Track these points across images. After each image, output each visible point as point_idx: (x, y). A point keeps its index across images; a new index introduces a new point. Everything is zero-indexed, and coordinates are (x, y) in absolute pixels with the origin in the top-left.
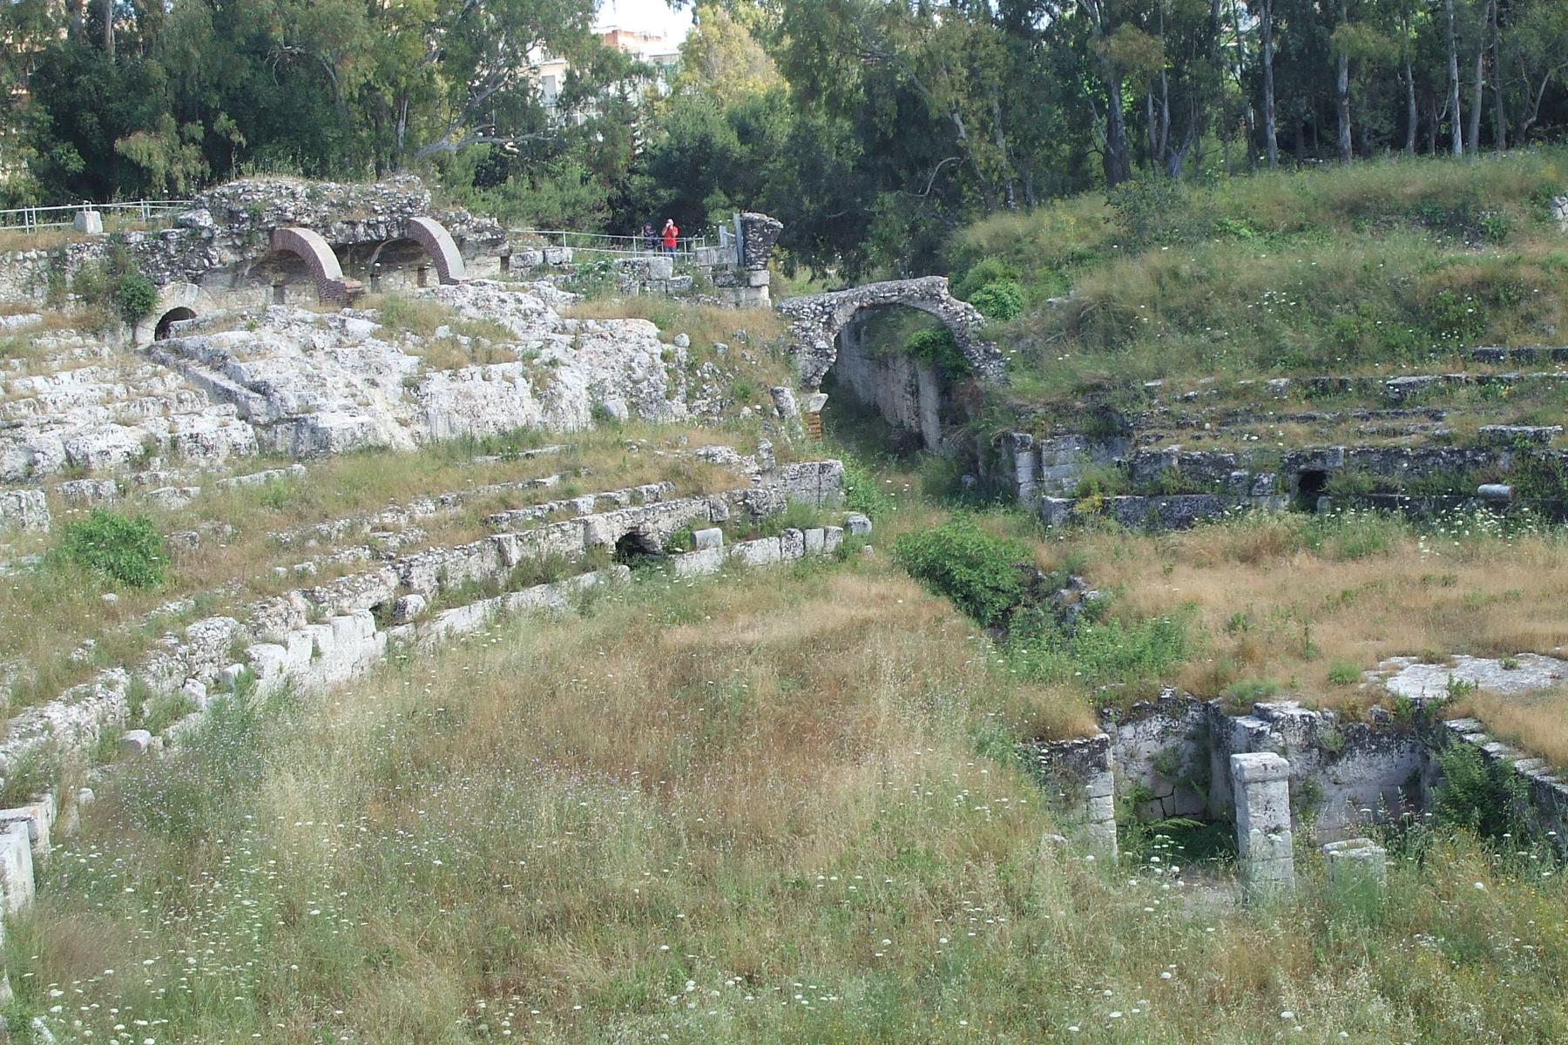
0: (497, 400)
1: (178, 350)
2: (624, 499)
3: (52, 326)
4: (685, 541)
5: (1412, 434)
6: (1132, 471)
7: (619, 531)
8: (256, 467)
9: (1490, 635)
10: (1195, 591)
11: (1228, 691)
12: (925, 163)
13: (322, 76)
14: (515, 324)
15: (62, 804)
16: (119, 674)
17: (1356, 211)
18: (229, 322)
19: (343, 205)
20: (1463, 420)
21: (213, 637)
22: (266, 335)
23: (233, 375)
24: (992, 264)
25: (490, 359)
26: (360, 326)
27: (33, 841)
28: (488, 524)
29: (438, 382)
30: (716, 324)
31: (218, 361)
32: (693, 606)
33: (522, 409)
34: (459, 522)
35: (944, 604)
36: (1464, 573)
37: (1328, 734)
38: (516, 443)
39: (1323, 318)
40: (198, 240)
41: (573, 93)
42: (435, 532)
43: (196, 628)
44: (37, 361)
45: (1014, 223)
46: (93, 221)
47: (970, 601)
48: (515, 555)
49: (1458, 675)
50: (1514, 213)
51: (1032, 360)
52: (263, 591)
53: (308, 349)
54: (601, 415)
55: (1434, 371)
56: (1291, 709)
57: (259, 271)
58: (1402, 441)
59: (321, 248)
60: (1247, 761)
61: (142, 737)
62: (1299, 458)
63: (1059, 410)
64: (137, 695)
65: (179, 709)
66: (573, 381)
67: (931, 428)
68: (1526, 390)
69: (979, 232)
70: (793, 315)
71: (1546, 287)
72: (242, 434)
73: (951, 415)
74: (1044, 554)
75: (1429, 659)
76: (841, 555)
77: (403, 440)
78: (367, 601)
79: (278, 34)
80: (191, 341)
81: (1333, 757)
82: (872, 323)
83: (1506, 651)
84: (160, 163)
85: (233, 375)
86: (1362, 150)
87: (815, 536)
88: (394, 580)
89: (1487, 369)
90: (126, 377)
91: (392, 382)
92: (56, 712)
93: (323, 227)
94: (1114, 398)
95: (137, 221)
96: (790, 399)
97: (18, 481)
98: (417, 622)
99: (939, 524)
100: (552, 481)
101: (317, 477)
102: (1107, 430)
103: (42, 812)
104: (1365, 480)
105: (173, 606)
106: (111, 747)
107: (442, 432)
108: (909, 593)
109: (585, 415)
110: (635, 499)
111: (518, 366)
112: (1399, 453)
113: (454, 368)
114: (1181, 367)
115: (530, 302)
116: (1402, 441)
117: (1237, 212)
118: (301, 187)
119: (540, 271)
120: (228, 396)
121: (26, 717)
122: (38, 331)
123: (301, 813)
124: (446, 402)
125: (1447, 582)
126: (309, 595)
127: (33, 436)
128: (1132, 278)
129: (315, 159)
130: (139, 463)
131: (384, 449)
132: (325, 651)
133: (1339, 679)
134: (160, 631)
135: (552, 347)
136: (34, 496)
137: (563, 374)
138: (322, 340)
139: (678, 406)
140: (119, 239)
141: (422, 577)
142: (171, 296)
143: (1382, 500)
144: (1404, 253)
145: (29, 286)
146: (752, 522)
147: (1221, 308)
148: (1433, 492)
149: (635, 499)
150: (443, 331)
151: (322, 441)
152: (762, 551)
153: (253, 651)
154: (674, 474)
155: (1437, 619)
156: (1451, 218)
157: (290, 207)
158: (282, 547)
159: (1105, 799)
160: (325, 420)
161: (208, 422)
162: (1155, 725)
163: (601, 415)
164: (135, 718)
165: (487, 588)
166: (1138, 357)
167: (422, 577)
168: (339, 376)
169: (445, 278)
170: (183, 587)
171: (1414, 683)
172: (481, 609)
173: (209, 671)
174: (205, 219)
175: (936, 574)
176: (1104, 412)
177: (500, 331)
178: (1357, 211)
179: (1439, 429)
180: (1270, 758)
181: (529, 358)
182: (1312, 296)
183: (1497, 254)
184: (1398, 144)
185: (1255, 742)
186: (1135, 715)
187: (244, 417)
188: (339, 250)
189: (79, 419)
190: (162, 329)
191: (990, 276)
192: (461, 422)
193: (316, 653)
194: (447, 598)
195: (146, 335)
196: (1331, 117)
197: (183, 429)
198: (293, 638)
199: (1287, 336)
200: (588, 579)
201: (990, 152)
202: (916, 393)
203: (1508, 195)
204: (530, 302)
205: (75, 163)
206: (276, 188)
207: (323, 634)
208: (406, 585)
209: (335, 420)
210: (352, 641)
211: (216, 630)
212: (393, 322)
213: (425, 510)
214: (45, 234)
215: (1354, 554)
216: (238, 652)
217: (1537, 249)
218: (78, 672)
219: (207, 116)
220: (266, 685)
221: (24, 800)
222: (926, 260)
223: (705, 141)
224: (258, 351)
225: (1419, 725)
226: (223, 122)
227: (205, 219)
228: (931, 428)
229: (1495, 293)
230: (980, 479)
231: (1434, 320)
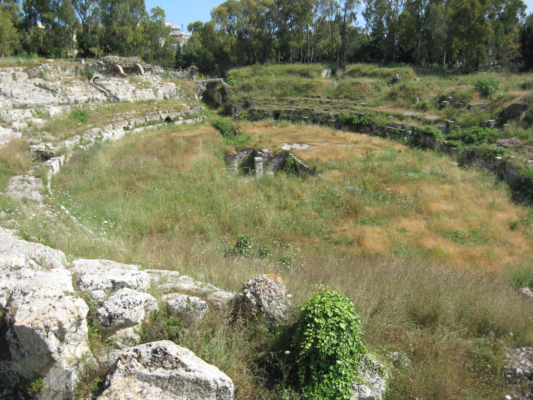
0: (148, 95)
1: (96, 84)
2: (167, 112)
3: (75, 79)
4: (177, 119)
5: (294, 108)
6: (250, 112)
7: (166, 117)
8: (106, 103)
9: (300, 141)
10: (255, 132)
11: (257, 147)
12: (223, 60)
13: (124, 40)
14: (152, 82)
15: (66, 157)
16: (79, 137)
17: (290, 72)
18: (104, 80)
19: (125, 61)
20: (302, 106)
21: (95, 131)
22: (110, 82)
23: (104, 88)
24: (232, 77)
25: (147, 88)
26: (126, 81)
27: (60, 163)
28: (144, 115)
29: (138, 91)
30: (185, 84)
31: (101, 85)
32: (177, 129)
33: (153, 97)
34: (139, 114)
35: (218, 133)
36: (298, 131)
37: (272, 156)
38: (150, 102)
39: (282, 89)
40: (100, 65)
41: (166, 45)
42: (135, 116)
43: (93, 129)
44: (71, 84)
45: (235, 70)
46: (83, 62)
47: (222, 132)
48: (148, 120)
49: (293, 147)
50: (315, 74)
51: (236, 93)
52: (105, 124)
53: (117, 85)
54: (165, 98)
55: (298, 98)
56: (266, 151)
57: (110, 72)
58: (292, 109)
59: (121, 68)
60: (257, 158)
61: (82, 147)
62: (275, 111)
63: (239, 101)
64: (81, 140)
65: (89, 142)
66: (161, 92)
67: (221, 103)
68: (312, 102)
69: (230, 72)
70: (198, 83)
71: (317, 86)
72: (105, 98)
73: (224, 101)
74: (234, 124)
75: (289, 144)
76: (202, 123)
77: (132, 100)
78: (123, 126)
79: (117, 32)
80: (98, 82)
81: (272, 158)
82: (211, 86)
83: (301, 143)
84: (96, 52)
85: (104, 88)
86: (294, 63)
87: (198, 119)
88: (127, 123)
89: (306, 98)
90: (86, 88)
91: (130, 91)
92: (67, 142)
93: (121, 65)
94: (248, 100)
95: (91, 62)
96: (196, 97)
97: (67, 104)
98: (131, 130)
99: (218, 118)
100: (155, 108)
101: (116, 106)
102: (247, 105)
103: (62, 158)
104: (286, 115)
105: (89, 126)
106: (76, 148)
107: (138, 99)
108: (212, 129)
109: (162, 98)
110: (169, 112)
111: (151, 90)
112: (290, 111)
113: (141, 89)
114: (259, 95)
115: (155, 79)
116: (292, 109)
117: (271, 71)
118: (118, 58)
119: (157, 74)
120: (103, 92)
121: (62, 143)
122: (72, 79)
123: (103, 160)
124: (139, 95)
125: (295, 132)
126: (113, 125)
127: (69, 97)
128: (252, 81)
129: (121, 54)
130: (87, 102)
131: (128, 102)
132: (115, 134)
133: (274, 146)
134: (87, 130)
135: (158, 86)
136: (68, 107)
137: (159, 91)
138: (119, 83)
139: (178, 97)
140: (87, 65)
141: (132, 123)
142: (96, 75)
143: (288, 118)
144: (295, 79)
145: (72, 72)
146: (188, 116)
147: (266, 86)
148: (296, 117)
149: (169, 112)
150: (140, 83)
151: (118, 99)
152: (189, 121)
153: (103, 133)
154: (175, 108)
155: (291, 138)
156: (304, 74)
157: (116, 61)
158: (109, 117)
159: (236, 164)
160: (119, 97)
161: (99, 96)
163: (165, 98)
164: (81, 143)
165: (143, 125)
166: (252, 93)
167: (132, 123)
168: (122, 89)
169: (141, 74)
170: (92, 123)
171: (286, 147)
172: (142, 129)
173: (95, 137)
174: (102, 62)
175: (216, 126)
176: (246, 102)
177: (149, 83)
178: (290, 72)
179: (298, 107)
180: (260, 158)
181: (154, 88)
182: (280, 85)
183: (310, 80)
184: (298, 61)
185: (260, 156)
186: (243, 151)
187: (106, 95)
188: (124, 69)
189: (77, 94)
190: (94, 80)
191: (231, 79)
192: (142, 98)
193: (113, 134)
194: (136, 126)
195: (91, 81)
196: (289, 57)
197: (95, 97)
198: (109, 132)
199: (276, 91)
200: (160, 125)
201: (233, 58)
202: (219, 97)
203: (314, 71)
204: (155, 79)
205: (83, 52)
206: (114, 58)
207: (115, 131)
208: (129, 124)
209: (120, 97)
210: (120, 133)
211: (96, 130)
212: (131, 81)
213: (134, 112)
214: (76, 63)
215: (282, 127)
216: (100, 134)
217: (316, 80)
218: (72, 136)
219: (105, 45)
220: (104, 140)
221: (59, 156)
222: (223, 76)
223: (191, 54)
224: (109, 85)
225: (286, 154)
226: (108, 46)
227: (102, 62)
228: (221, 103)
229: (308, 87)
230: (227, 112)
231: (298, 90)
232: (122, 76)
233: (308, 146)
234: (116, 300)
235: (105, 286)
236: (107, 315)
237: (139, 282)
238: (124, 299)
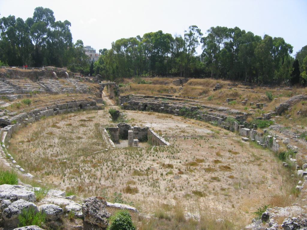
60: (129, 131)
93: (56, 72)
119: (77, 78)
120: (43, 87)
162: (124, 127)
171: (148, 125)
209: (54, 90)
232: (57, 79)
233: (162, 125)
234: (15, 205)
235: (11, 198)
236: (9, 212)
237: (30, 197)
238: (19, 205)
